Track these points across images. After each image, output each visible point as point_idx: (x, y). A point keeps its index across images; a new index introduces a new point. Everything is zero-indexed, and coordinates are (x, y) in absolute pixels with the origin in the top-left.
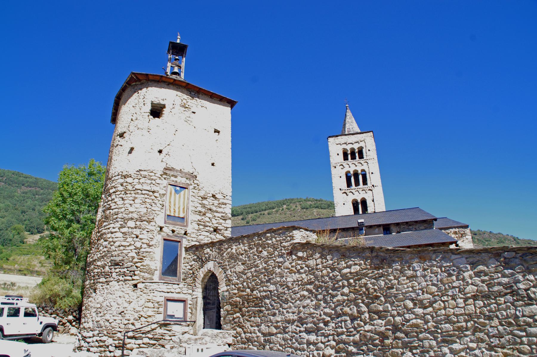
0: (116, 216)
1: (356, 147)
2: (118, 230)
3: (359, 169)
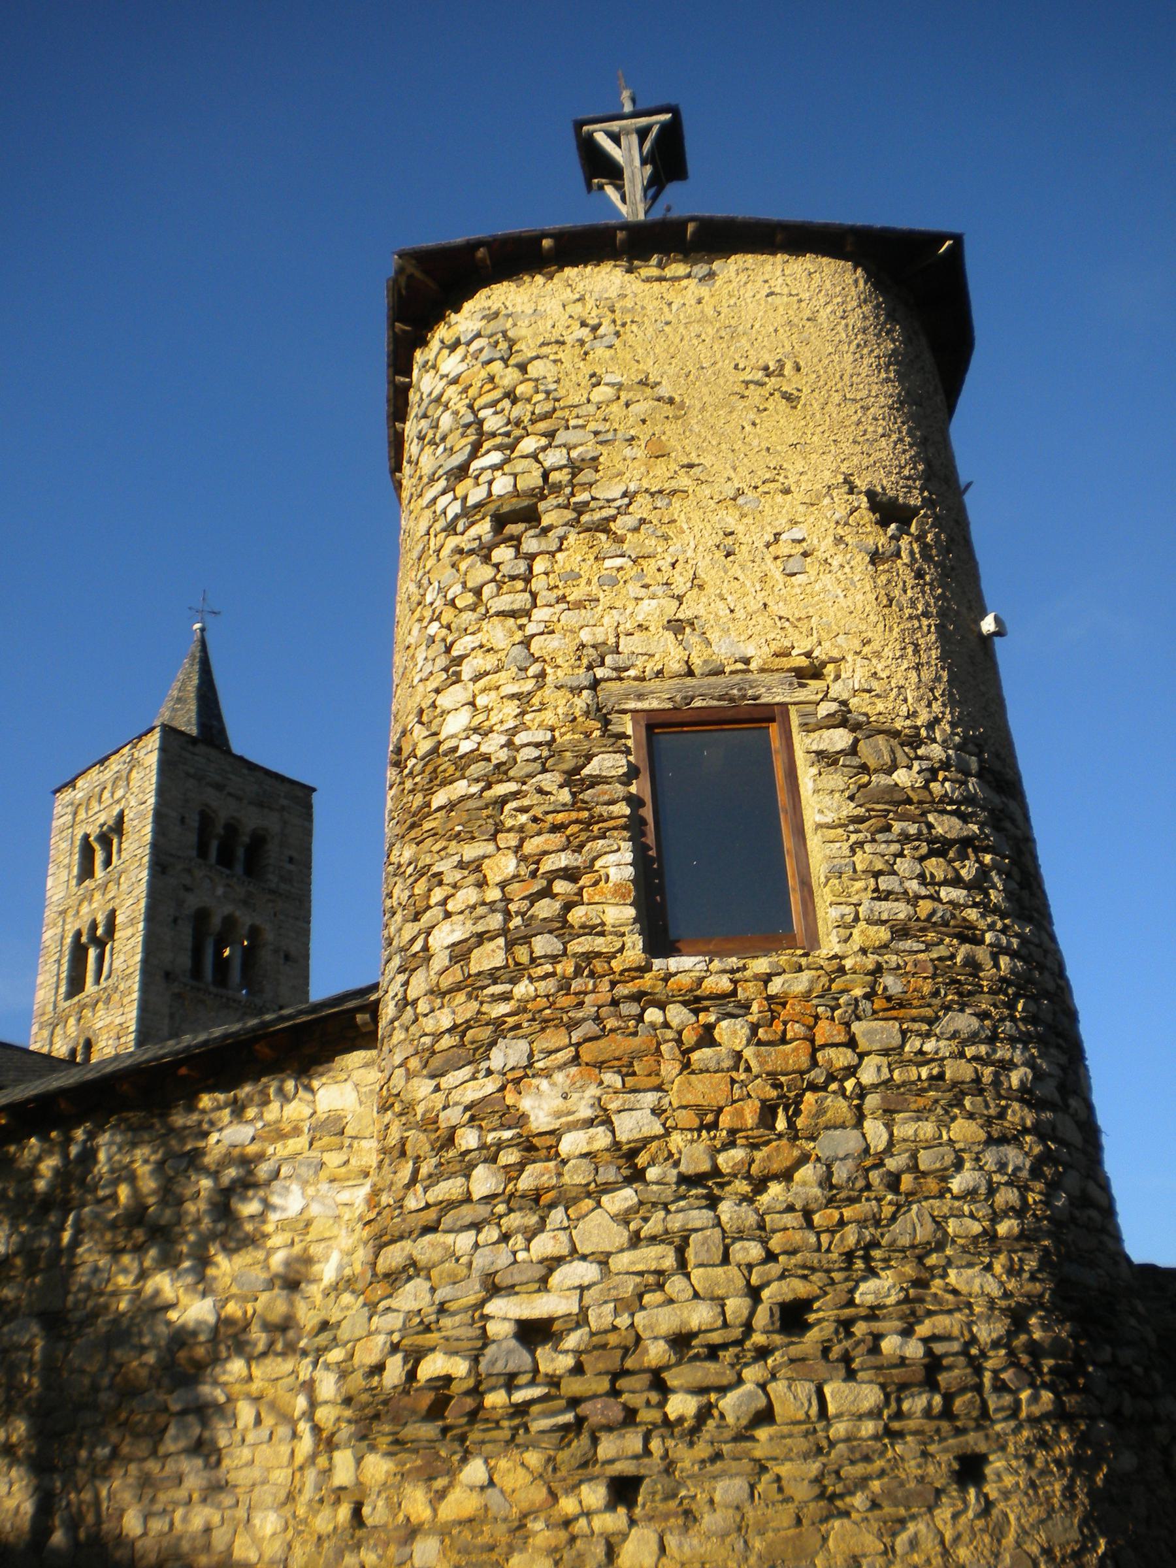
1: (252, 820)
3: (246, 919)
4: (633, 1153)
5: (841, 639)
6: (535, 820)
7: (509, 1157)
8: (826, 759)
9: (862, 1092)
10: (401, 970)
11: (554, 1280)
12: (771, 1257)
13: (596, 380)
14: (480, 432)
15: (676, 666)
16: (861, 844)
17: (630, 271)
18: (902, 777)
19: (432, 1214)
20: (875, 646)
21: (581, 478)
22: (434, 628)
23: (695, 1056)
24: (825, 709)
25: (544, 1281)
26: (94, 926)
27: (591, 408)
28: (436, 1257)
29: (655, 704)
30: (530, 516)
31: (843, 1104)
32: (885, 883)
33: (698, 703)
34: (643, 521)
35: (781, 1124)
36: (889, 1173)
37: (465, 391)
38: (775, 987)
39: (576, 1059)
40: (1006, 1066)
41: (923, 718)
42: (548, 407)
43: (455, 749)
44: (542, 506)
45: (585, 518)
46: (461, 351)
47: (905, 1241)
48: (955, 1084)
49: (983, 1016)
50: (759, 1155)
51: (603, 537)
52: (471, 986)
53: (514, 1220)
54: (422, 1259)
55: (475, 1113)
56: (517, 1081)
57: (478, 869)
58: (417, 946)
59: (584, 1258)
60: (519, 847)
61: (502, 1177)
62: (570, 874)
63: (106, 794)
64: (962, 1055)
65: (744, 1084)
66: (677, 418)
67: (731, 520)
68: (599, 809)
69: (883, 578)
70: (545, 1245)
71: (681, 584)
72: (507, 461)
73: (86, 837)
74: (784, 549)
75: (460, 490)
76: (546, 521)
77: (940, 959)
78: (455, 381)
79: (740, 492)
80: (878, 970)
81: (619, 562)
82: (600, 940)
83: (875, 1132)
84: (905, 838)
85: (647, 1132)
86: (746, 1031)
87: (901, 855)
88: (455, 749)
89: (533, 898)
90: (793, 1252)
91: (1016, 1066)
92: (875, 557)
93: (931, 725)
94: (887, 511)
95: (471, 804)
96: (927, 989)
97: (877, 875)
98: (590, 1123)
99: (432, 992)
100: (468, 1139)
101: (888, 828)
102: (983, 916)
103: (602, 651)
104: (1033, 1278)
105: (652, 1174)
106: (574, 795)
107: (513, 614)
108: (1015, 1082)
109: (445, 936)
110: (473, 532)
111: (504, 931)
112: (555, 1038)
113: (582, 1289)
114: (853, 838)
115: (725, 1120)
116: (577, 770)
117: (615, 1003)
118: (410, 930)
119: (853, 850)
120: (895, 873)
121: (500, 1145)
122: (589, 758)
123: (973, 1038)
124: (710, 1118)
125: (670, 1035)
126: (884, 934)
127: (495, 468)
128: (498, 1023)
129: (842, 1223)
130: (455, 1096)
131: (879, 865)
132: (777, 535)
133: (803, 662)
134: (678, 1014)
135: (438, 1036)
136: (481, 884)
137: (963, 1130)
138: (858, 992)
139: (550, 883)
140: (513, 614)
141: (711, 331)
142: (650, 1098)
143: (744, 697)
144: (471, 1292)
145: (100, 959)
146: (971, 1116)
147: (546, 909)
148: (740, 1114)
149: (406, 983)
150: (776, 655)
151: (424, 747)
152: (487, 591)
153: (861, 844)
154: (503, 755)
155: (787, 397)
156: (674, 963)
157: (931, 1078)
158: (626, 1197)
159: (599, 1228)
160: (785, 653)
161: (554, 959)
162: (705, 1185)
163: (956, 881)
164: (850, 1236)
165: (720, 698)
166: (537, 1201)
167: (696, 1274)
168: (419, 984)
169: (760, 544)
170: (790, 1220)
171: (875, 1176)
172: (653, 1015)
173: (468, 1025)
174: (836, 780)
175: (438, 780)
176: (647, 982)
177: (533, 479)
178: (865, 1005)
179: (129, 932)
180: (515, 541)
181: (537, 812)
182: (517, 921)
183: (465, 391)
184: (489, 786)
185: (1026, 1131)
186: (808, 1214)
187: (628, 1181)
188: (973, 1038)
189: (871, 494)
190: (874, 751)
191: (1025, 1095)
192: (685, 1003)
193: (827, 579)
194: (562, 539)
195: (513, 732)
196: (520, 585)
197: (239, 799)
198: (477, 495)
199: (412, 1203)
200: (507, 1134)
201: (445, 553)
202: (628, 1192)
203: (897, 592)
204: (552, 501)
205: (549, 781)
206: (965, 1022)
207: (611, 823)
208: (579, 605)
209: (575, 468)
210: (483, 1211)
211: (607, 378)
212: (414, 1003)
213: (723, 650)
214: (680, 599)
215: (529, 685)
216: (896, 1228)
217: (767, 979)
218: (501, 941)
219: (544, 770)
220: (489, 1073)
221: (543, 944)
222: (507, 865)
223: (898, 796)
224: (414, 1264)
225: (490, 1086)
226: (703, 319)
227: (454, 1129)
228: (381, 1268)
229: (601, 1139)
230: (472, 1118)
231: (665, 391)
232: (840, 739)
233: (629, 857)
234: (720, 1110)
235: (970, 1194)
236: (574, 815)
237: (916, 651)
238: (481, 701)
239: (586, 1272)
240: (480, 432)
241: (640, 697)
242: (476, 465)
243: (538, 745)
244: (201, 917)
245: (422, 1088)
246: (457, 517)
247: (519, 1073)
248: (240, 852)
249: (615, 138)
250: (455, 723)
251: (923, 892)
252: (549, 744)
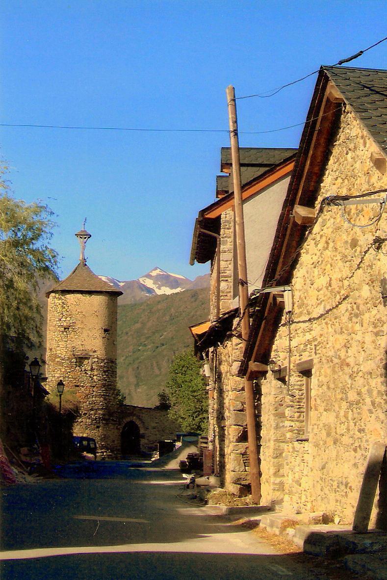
24: (96, 356)
32: (98, 375)
94: (106, 331)
136: (61, 371)
198: (62, 324)
204: (71, 327)
206: (103, 389)
221: (66, 379)
250: (59, 352)
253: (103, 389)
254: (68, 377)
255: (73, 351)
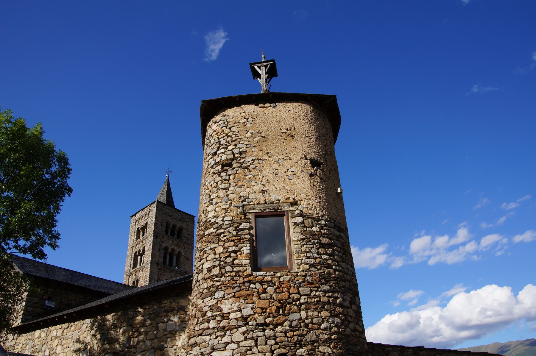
0: (344, 284)
1: (179, 225)
2: (349, 305)
3: (177, 249)
4: (247, 318)
5: (301, 195)
6: (227, 239)
7: (218, 318)
8: (296, 224)
9: (301, 304)
10: (197, 273)
11: (227, 348)
12: (276, 343)
13: (247, 132)
14: (220, 144)
15: (262, 202)
16: (303, 245)
17: (256, 105)
18: (314, 229)
19: (201, 332)
20: (310, 197)
21: (242, 156)
22: (207, 191)
23: (261, 296)
24: (297, 212)
25: (225, 347)
26: (140, 251)
27: (246, 139)
28: (201, 342)
29: (257, 211)
30: (230, 165)
31: (296, 307)
32: (309, 254)
33: (267, 211)
34: (256, 166)
35: (281, 312)
36: (306, 324)
37: (217, 134)
38: (281, 280)
39: (234, 296)
40: (337, 298)
41: (321, 214)
42: (235, 138)
43: (210, 221)
44: (233, 162)
45: (243, 166)
46: (217, 124)
47: (309, 340)
48: (323, 302)
49: (330, 286)
50: (275, 319)
51: (247, 170)
52: (211, 278)
53: (219, 333)
54: (198, 342)
55: (212, 308)
56: (221, 301)
57: (214, 250)
58: (200, 268)
59: (234, 343)
60: (224, 245)
61: (217, 323)
62: (235, 252)
63: (143, 218)
64: (325, 296)
65: (272, 302)
66: (265, 141)
67: (277, 167)
68: (242, 236)
69: (312, 180)
70: (225, 339)
71: (264, 182)
72: (225, 151)
73: (138, 228)
74: (289, 173)
75: (215, 158)
76: (234, 166)
77: (321, 273)
78: (215, 131)
79: (279, 159)
80: (306, 276)
81: (250, 176)
82: (241, 268)
83: (303, 314)
84: (314, 243)
85: (250, 313)
86: (274, 290)
87: (313, 247)
88: (210, 221)
89: (226, 257)
90: (282, 342)
91: (339, 298)
92: (311, 175)
93: (322, 216)
94: (314, 163)
95: (213, 234)
96: (317, 279)
97: (307, 252)
98: (237, 311)
99: (203, 279)
100: (209, 314)
101: (310, 241)
102: (333, 262)
103: (245, 198)
104: (340, 349)
105: (250, 323)
106: (237, 233)
107: (225, 189)
108: (338, 301)
109: (207, 265)
110: (217, 168)
111: (219, 265)
112: (229, 291)
113: (233, 350)
114: (302, 244)
115: (268, 311)
116: (238, 227)
117: (244, 283)
118: (199, 264)
119: (301, 247)
120: (311, 252)
121: (216, 316)
122: (241, 224)
123: (328, 292)
124: (264, 310)
125: (256, 290)
126: (307, 267)
127: (223, 153)
128: (217, 287)
129: (294, 335)
130: (207, 304)
131: (307, 250)
132: (288, 170)
133: (292, 201)
134: (258, 286)
135: (204, 289)
136: (215, 254)
137: (324, 313)
138: (301, 281)
139: (230, 254)
140: (225, 189)
141: (275, 120)
142: (251, 305)
143: (278, 209)
144: (208, 350)
145: (141, 259)
146: (326, 310)
147: (229, 260)
148: (271, 310)
149: (198, 276)
150: (286, 199)
151: (204, 220)
152: (219, 183)
153: (303, 245)
154: (221, 223)
155: (292, 136)
156: (258, 273)
157: (317, 301)
158: (244, 329)
159: (237, 336)
160: (288, 198)
161: (230, 272)
162: (263, 326)
163: (326, 254)
164: (296, 338)
165: (272, 209)
166: (224, 329)
167: (259, 347)
168: (200, 277)
169: (284, 172)
170: (281, 335)
171: (302, 324)
172: (252, 286)
173: (210, 287)
174: (298, 230)
175: (206, 228)
176: (251, 278)
177: (232, 156)
178: (303, 284)
179: (148, 253)
180: (227, 170)
181: (228, 237)
182: (222, 263)
183: (217, 134)
184: (218, 230)
185: (340, 314)
186: (286, 333)
187: (245, 325)
188: (328, 292)
189: (310, 159)
190: (308, 222)
191: (341, 305)
192: (260, 283)
193: (299, 181)
194: (237, 171)
195: (224, 217)
196: (227, 182)
197: (176, 219)
198: (218, 160)
199: (196, 329)
200: (218, 313)
201: (211, 173)
202: (245, 327)
203: (316, 184)
204: (235, 161)
205: (231, 229)
206: (326, 287)
207: (245, 240)
208: (240, 187)
209: (241, 153)
210: (212, 331)
211: (250, 131)
212: (199, 281)
213: (274, 198)
214: (264, 185)
215: (228, 206)
216: (307, 337)
217: (279, 277)
218: (218, 267)
219: (230, 227)
220: (215, 299)
221: (228, 268)
222: (220, 249)
223: (313, 233)
224: (196, 343)
225: (214, 302)
226: (273, 117)
227: (206, 312)
228: (189, 344)
229: (239, 315)
230: (210, 309)
231: (263, 135)
232: (300, 219)
233: (249, 248)
234: (267, 308)
235: (325, 329)
236: (236, 238)
237: (320, 198)
238: (217, 210)
239: (234, 346)
240: (220, 144)
241: (254, 209)
242: (218, 152)
243: (229, 221)
244: (166, 249)
245: (200, 302)
246: (214, 164)
247: (221, 299)
248: (176, 232)
249: (259, 67)
250: (211, 215)
251: (318, 256)
252: (232, 220)
253: (326, 287)
254: (233, 265)
255: (243, 206)
